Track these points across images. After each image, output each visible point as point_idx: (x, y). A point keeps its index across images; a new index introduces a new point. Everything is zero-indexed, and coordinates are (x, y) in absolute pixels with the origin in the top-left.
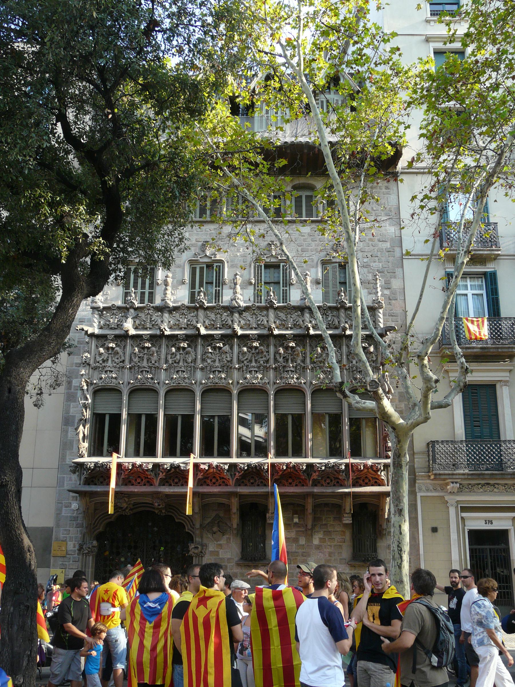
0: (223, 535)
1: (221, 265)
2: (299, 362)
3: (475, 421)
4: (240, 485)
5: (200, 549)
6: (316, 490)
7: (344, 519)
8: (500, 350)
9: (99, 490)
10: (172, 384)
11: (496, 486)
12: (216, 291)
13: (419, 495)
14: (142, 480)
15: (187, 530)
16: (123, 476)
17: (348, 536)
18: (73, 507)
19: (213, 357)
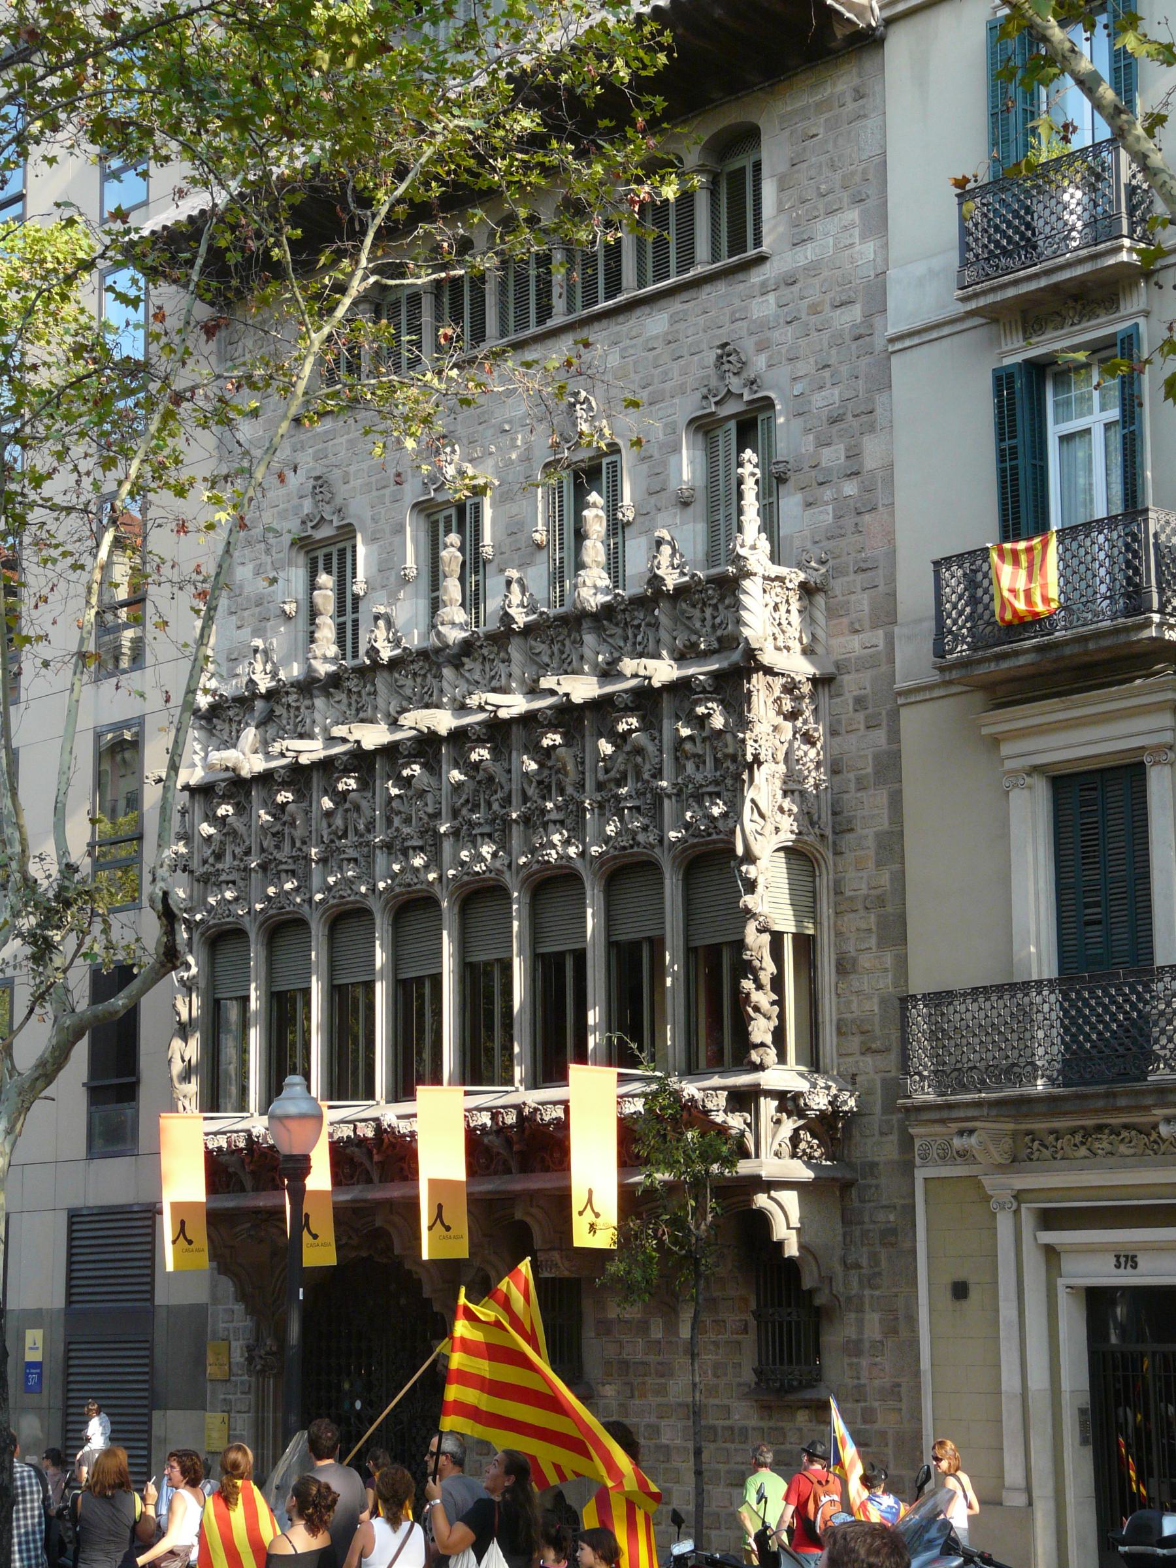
3: (1087, 906)
8: (1091, 646)
10: (332, 902)
11: (1124, 1134)
13: (920, 1174)
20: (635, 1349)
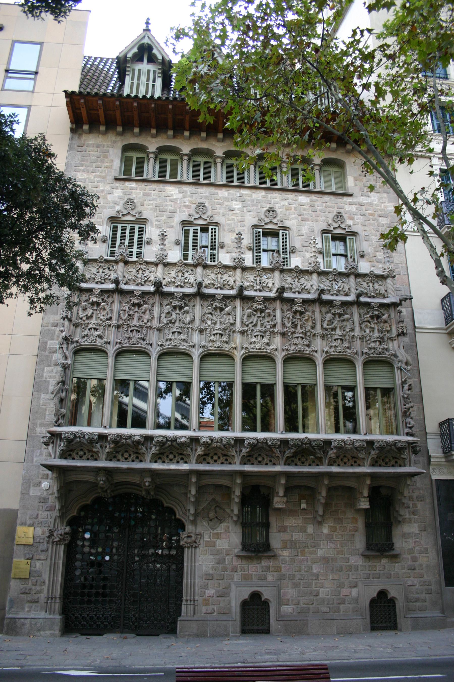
0: (221, 523)
1: (217, 228)
2: (309, 328)
4: (245, 464)
5: (193, 539)
6: (335, 469)
7: (362, 503)
12: (211, 254)
14: (130, 455)
15: (177, 516)
16: (107, 450)
17: (361, 524)
18: (43, 486)
19: (214, 318)
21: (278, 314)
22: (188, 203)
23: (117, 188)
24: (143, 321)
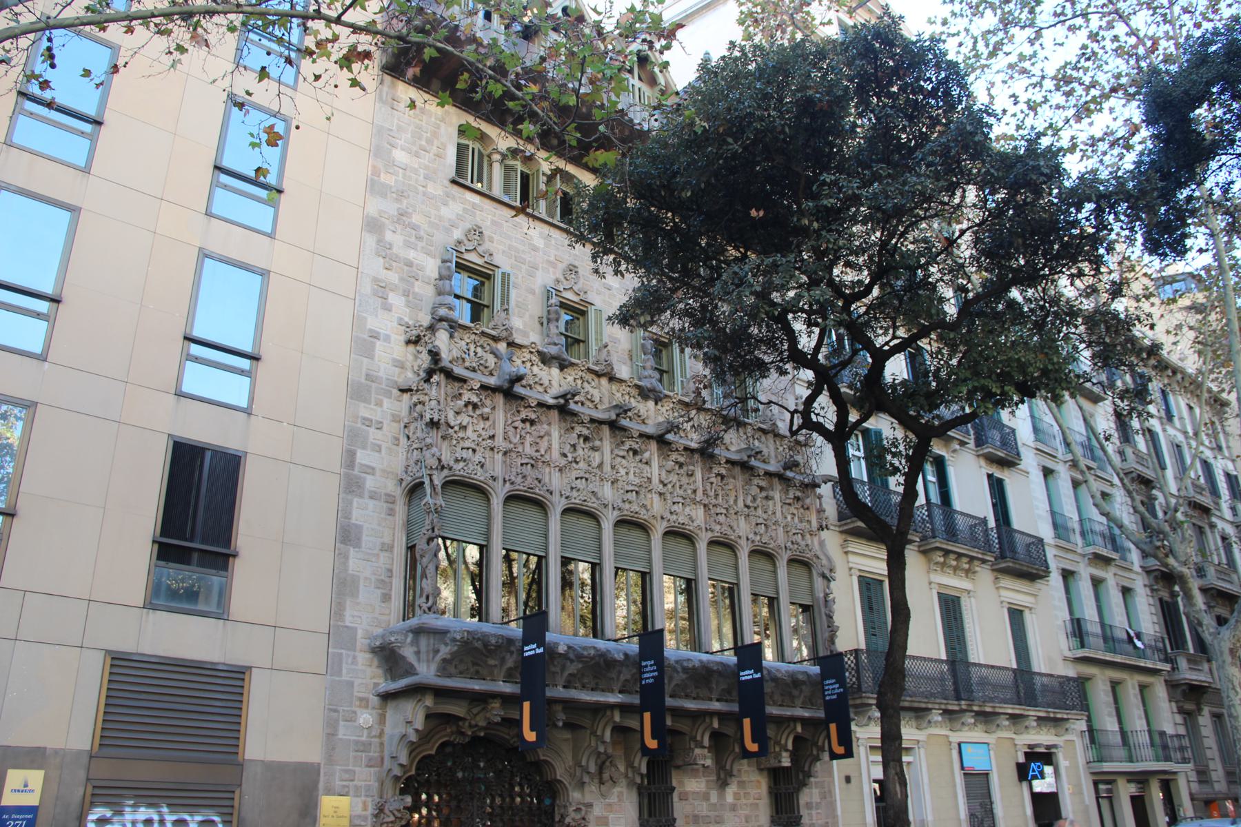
9: (477, 687)
18: (361, 721)
20: (702, 809)
21: (699, 475)
22: (552, 259)
23: (454, 198)
24: (537, 451)
